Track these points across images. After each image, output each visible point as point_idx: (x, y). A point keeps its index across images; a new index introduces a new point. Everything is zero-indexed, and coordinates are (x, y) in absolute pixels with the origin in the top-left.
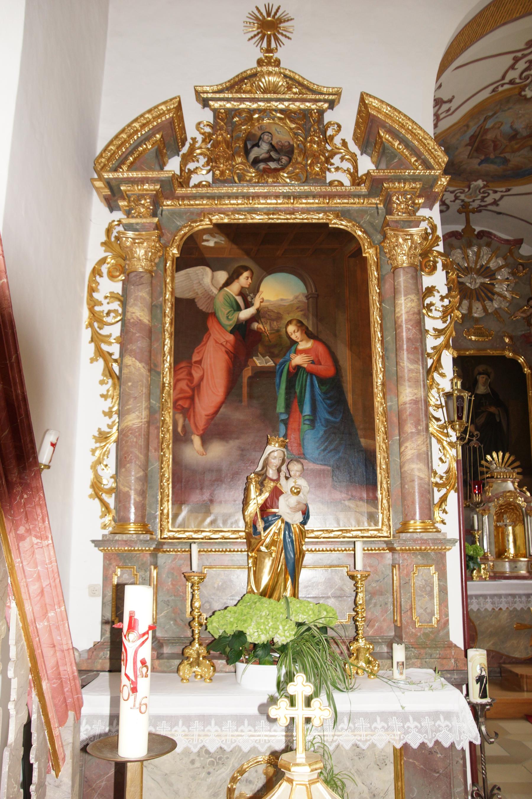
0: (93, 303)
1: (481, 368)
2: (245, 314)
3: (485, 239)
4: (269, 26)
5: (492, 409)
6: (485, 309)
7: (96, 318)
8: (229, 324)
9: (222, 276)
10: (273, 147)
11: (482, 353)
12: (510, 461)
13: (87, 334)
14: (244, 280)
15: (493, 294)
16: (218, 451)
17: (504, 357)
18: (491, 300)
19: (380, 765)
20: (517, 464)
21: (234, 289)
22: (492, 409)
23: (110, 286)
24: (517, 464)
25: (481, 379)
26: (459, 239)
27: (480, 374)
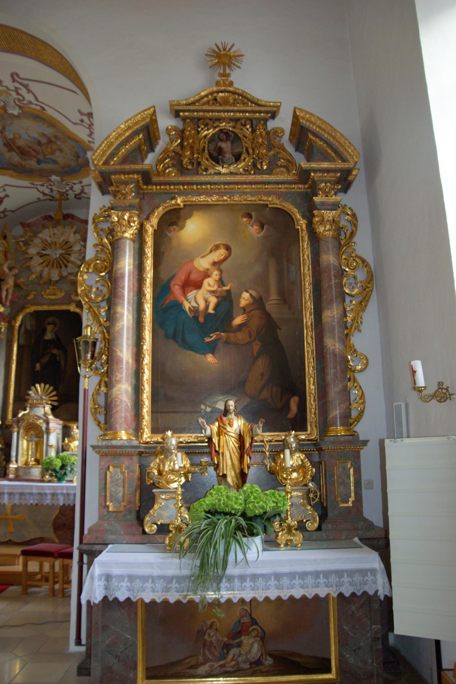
1: (50, 320)
3: (69, 220)
5: (55, 351)
11: (52, 308)
12: (49, 391)
15: (68, 262)
17: (68, 311)
18: (66, 266)
20: (54, 393)
22: (55, 351)
24: (54, 393)
25: (50, 328)
26: (50, 221)
27: (51, 324)
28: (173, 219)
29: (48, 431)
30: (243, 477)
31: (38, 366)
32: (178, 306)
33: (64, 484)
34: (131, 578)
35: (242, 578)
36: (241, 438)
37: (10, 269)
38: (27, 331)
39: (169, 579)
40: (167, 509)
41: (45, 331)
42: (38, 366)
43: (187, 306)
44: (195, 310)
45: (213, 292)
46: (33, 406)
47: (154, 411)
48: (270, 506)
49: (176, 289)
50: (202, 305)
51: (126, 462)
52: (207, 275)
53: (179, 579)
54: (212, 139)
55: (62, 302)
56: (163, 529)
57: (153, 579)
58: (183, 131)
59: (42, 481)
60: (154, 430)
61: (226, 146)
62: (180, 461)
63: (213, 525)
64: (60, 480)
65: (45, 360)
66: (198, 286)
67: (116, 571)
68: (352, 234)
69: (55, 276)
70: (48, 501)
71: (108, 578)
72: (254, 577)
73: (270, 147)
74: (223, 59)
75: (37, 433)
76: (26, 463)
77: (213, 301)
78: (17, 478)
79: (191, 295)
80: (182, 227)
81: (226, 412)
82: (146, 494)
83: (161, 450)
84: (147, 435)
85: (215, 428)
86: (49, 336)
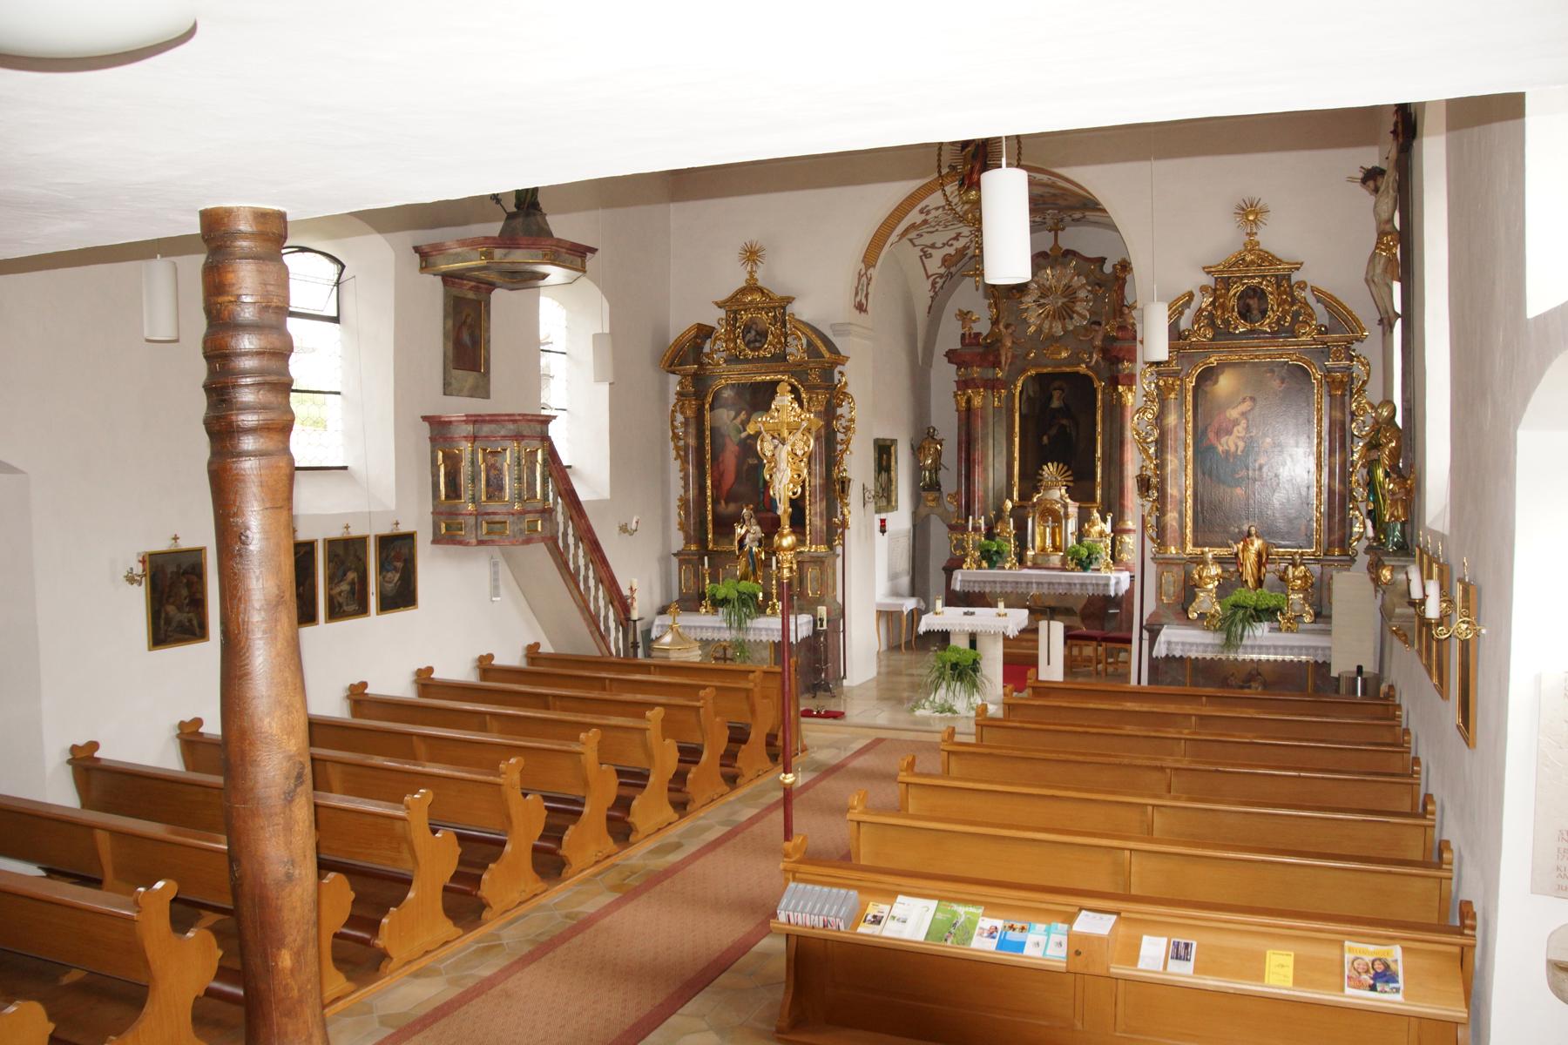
0: (674, 428)
1: (1057, 384)
2: (743, 435)
4: (752, 255)
5: (1064, 422)
6: (1064, 328)
7: (676, 437)
8: (736, 440)
9: (732, 414)
10: (758, 333)
13: (672, 445)
14: (743, 416)
16: (732, 507)
17: (1077, 373)
19: (765, 647)
21: (738, 421)
22: (1064, 422)
23: (680, 418)
25: (1056, 394)
28: (1208, 376)
29: (1067, 516)
30: (1260, 583)
31: (1045, 439)
32: (1212, 448)
33: (1089, 574)
34: (1183, 644)
35: (1253, 647)
36: (1259, 555)
37: (1007, 326)
38: (1029, 398)
39: (1207, 645)
40: (1206, 601)
41: (1051, 397)
42: (1045, 439)
43: (1220, 449)
44: (1227, 452)
45: (1242, 438)
46: (1048, 488)
47: (1195, 531)
48: (1273, 603)
49: (1211, 435)
50: (1233, 449)
51: (1175, 569)
52: (1236, 423)
53: (1214, 645)
54: (1242, 296)
55: (1071, 361)
56: (1202, 616)
57: (1197, 645)
58: (1215, 290)
59: (1063, 569)
60: (1195, 545)
61: (1253, 303)
62: (1215, 570)
63: (1234, 614)
64: (1085, 569)
65: (1053, 431)
66: (1229, 432)
67: (1174, 639)
68: (1365, 383)
69: (1058, 329)
70: (1076, 591)
71: (1169, 643)
72: (1260, 647)
73: (1294, 301)
74: (1250, 213)
75: (1055, 517)
76: (1043, 549)
77: (1241, 444)
78: (1035, 566)
79: (1223, 440)
80: (1216, 382)
81: (1249, 535)
82: (1189, 591)
83: (1200, 561)
84: (1190, 548)
85: (1240, 546)
86: (1055, 404)
